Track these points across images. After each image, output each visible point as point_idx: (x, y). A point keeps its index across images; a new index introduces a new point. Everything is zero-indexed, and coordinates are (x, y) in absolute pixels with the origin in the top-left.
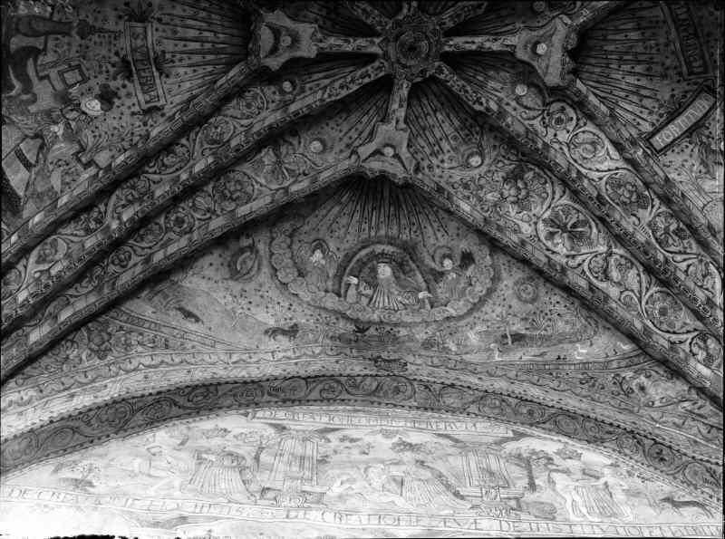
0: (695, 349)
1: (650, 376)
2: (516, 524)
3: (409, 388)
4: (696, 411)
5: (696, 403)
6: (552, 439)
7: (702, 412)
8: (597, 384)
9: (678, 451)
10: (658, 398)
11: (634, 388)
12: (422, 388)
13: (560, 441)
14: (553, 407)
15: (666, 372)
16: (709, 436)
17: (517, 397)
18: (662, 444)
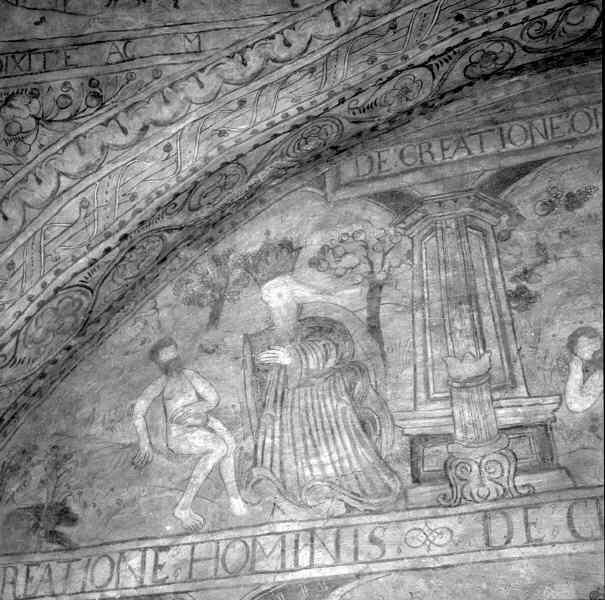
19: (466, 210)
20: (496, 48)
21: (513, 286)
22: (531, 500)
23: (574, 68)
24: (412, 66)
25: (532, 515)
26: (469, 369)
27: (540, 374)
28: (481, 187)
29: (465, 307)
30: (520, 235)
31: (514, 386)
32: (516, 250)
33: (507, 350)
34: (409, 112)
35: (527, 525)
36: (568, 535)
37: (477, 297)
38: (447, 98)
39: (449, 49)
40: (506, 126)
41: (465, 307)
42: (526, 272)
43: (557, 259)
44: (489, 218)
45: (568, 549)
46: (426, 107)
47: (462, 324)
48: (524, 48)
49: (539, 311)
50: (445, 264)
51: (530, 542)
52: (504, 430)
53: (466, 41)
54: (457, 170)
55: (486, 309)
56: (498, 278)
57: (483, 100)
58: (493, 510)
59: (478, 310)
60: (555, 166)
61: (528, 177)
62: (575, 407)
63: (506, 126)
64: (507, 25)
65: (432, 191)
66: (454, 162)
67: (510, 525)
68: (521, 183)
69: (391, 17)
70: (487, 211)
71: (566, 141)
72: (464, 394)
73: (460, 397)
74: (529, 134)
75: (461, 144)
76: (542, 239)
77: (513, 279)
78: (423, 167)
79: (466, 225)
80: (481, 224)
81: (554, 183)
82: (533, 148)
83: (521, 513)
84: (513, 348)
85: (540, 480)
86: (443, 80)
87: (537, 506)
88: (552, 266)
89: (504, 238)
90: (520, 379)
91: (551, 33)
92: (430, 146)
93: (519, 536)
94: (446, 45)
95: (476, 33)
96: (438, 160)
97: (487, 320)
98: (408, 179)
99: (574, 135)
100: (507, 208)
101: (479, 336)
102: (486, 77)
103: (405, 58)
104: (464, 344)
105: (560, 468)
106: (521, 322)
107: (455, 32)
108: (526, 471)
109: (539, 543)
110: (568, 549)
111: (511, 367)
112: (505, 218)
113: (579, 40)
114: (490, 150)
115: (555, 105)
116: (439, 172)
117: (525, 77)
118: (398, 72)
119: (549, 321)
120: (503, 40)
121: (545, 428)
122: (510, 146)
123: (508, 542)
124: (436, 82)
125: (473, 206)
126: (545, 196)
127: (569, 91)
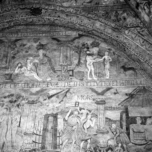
0: (145, 8)
1: (128, 14)
2: (70, 83)
3: (43, 20)
4: (141, 33)
5: (141, 29)
6: (91, 37)
7: (143, 33)
8: (108, 16)
9: (130, 50)
10: (129, 23)
11: (122, 18)
12: (47, 20)
13: (94, 38)
14: (91, 28)
15: (134, 13)
16: (143, 44)
17: (79, 24)
18: (125, 47)
19: (10, 44)
20: (18, 22)
21: (13, 56)
22: (7, 83)
23: (30, 26)
24: (4, 22)
25: (6, 85)
26: (4, 66)
27: (13, 68)
28: (13, 41)
29: (5, 58)
30: (16, 49)
31: (9, 68)
32: (15, 51)
33: (9, 64)
34: (5, 28)
35: (5, 86)
36: (10, 87)
37: (8, 56)
38: (11, 27)
39: (10, 21)
40: (18, 33)
41: (5, 58)
42: (15, 54)
43: (19, 53)
44: (12, 45)
45: (9, 89)
46: (8, 28)
47: (5, 60)
48: (22, 22)
49: (15, 59)
50: (5, 51)
51: (5, 88)
52: (6, 74)
53: (12, 20)
54: (10, 38)
55: (8, 58)
56: (11, 54)
57: (17, 28)
58: (2, 84)
59: (7, 58)
60: (23, 40)
61: (19, 41)
62: (16, 72)
63: (18, 33)
64: (18, 19)
65: (6, 41)
66: (10, 37)
67: (3, 85)
68: (18, 42)
69: (2, 14)
70: (12, 45)
71: (26, 37)
72: (2, 69)
73: (2, 70)
74: (21, 35)
75: (12, 34)
76: (19, 50)
77: (13, 55)
78: (5, 37)
79: (9, 46)
80: (11, 47)
81: (23, 42)
82: (21, 37)
83: (5, 84)
84: (10, 64)
85: (8, 81)
86: (10, 25)
87: (7, 84)
88: (19, 54)
89: (14, 49)
90: (10, 68)
91: (24, 21)
92: (7, 34)
93: (4, 87)
94: (9, 20)
95: (14, 19)
96: (8, 36)
97: (8, 60)
98: (3, 38)
99: (27, 36)
100: (15, 45)
101: (6, 62)
102: (17, 25)
103: (3, 21)
104: (4, 62)
105: (11, 79)
106: (12, 61)
107: (11, 18)
108: (7, 80)
109: (6, 88)
110: (9, 89)
111: (9, 66)
112: (15, 46)
113: (30, 22)
114: (15, 36)
115: (26, 31)
116: (8, 38)
117: (24, 26)
118: (2, 23)
119: (16, 61)
120: (18, 21)
121: (11, 74)
122: (18, 36)
123: (2, 88)
124: (9, 25)
125: (11, 44)
126: (21, 44)
127: (28, 29)
